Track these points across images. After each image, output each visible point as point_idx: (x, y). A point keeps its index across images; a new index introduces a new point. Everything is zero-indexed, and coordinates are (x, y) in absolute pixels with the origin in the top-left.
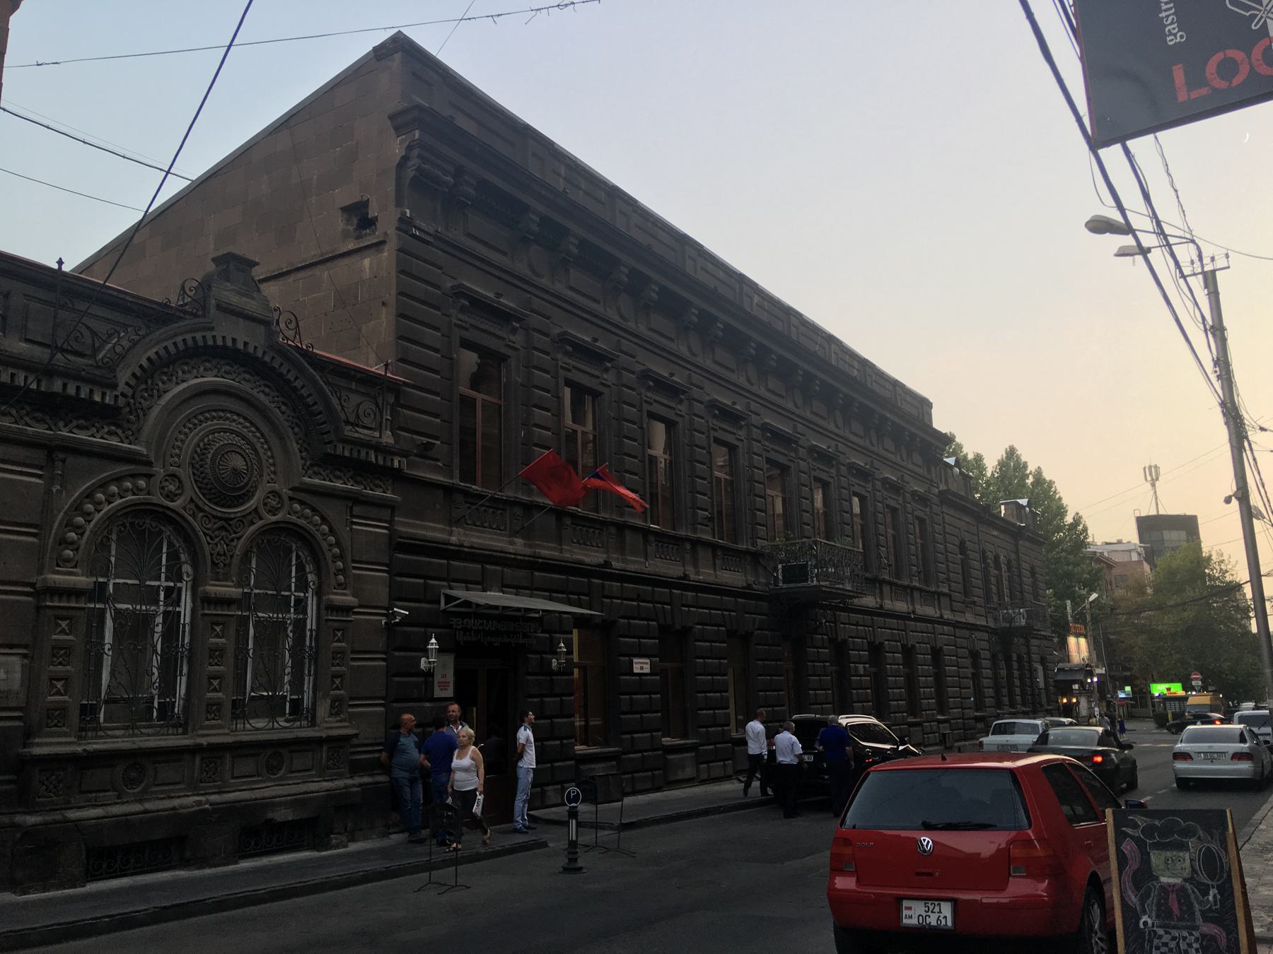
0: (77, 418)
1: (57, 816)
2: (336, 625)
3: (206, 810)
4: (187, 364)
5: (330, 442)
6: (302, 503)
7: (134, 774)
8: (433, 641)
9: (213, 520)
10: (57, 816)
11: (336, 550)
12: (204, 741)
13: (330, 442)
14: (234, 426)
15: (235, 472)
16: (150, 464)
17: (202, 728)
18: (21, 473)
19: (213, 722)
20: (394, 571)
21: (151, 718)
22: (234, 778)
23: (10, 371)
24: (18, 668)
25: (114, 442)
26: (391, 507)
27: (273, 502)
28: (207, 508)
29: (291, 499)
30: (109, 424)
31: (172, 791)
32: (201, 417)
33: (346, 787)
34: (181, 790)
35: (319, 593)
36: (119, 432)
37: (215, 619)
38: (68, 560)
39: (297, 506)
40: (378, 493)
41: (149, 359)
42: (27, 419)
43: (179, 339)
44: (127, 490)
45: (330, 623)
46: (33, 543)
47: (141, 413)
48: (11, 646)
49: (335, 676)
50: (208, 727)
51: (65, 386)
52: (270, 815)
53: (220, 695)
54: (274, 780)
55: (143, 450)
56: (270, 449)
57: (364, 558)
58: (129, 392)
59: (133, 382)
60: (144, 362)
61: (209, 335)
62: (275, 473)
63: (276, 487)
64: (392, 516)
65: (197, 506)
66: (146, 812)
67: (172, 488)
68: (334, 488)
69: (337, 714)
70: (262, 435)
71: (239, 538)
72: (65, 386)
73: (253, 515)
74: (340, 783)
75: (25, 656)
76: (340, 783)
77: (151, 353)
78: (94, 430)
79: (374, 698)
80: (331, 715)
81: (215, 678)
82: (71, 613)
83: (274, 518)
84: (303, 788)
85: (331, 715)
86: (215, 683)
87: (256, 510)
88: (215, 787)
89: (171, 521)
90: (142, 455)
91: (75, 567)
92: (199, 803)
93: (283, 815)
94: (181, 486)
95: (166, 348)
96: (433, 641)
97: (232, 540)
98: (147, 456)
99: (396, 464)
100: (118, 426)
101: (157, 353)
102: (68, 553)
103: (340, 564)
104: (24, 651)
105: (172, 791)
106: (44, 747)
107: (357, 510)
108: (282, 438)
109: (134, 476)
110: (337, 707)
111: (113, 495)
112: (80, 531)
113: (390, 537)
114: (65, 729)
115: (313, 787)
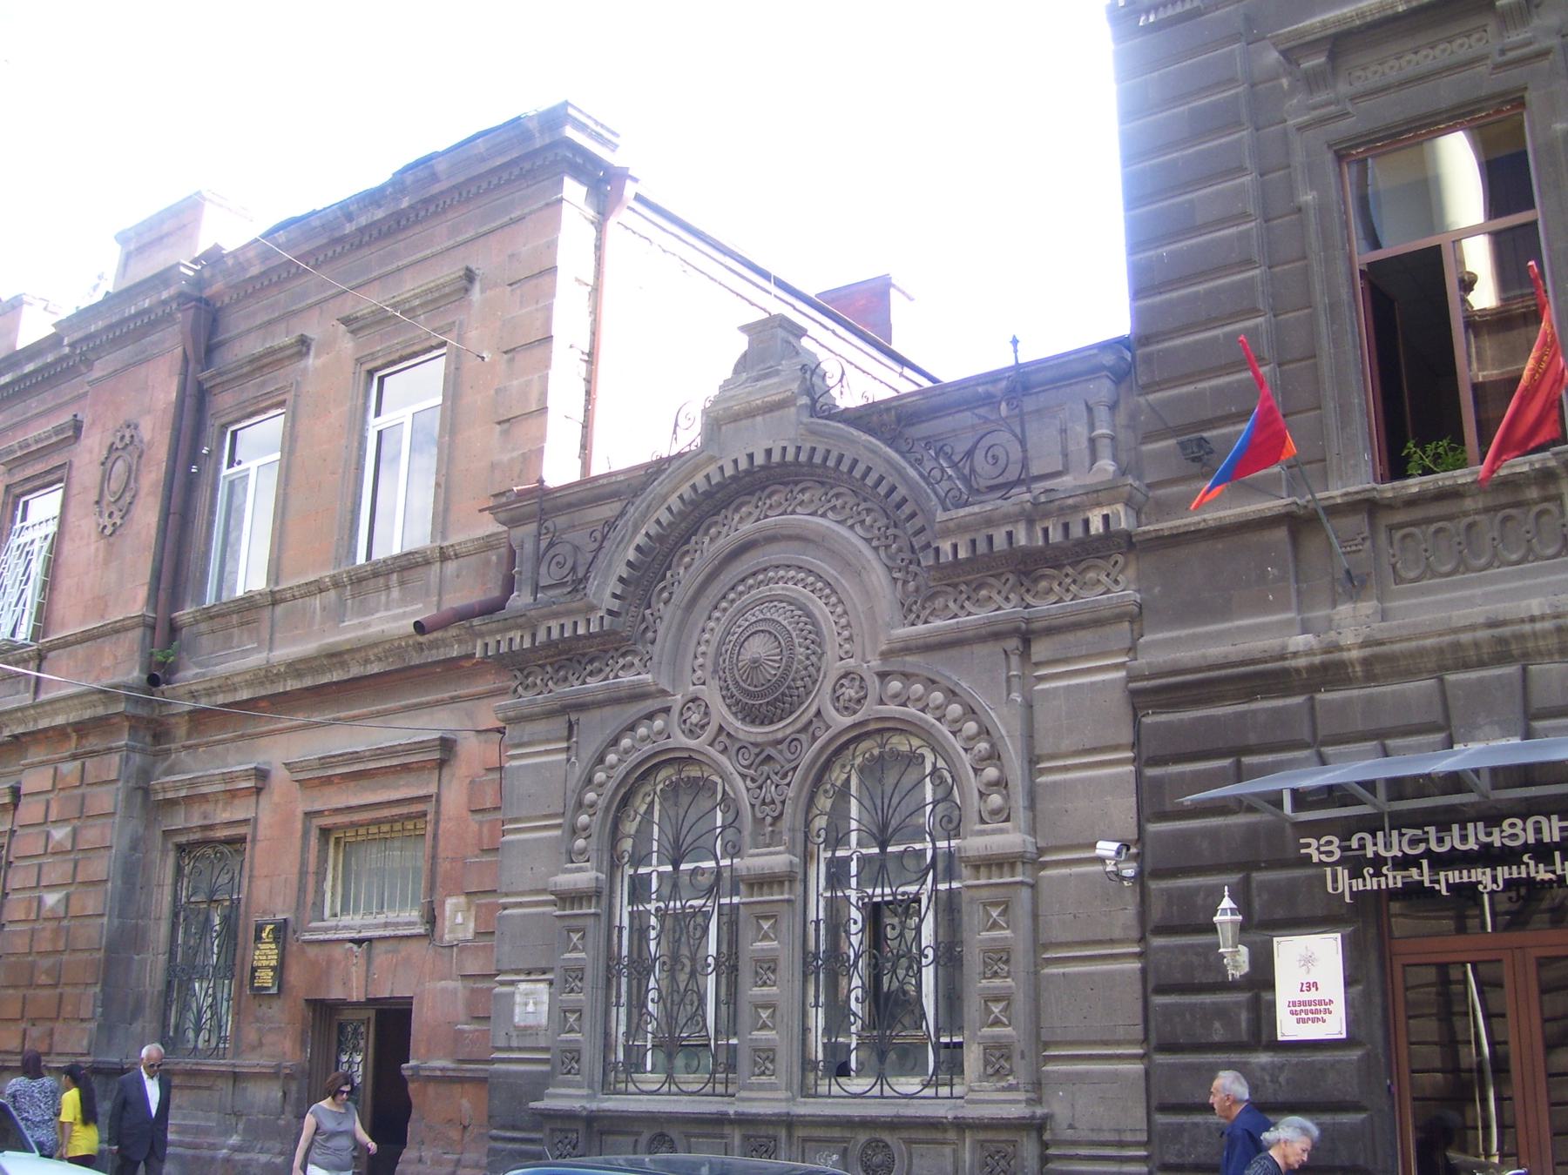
0: (591, 661)
5: (928, 545)
6: (906, 676)
8: (1227, 903)
14: (778, 589)
15: (756, 664)
16: (664, 693)
18: (547, 752)
24: (546, 998)
25: (627, 678)
27: (850, 693)
28: (741, 736)
29: (883, 676)
37: (759, 909)
39: (895, 685)
40: (1092, 597)
43: (673, 501)
50: (750, 1088)
55: (648, 677)
57: (1065, 745)
60: (631, 555)
62: (850, 639)
65: (729, 734)
67: (695, 718)
68: (959, 628)
71: (795, 769)
77: (640, 539)
79: (1118, 1043)
80: (986, 1077)
82: (579, 922)
83: (848, 720)
85: (986, 1077)
87: (818, 713)
96: (1227, 903)
97: (785, 776)
99: (1097, 526)
100: (634, 653)
101: (647, 534)
107: (1040, 650)
109: (650, 716)
110: (998, 1058)
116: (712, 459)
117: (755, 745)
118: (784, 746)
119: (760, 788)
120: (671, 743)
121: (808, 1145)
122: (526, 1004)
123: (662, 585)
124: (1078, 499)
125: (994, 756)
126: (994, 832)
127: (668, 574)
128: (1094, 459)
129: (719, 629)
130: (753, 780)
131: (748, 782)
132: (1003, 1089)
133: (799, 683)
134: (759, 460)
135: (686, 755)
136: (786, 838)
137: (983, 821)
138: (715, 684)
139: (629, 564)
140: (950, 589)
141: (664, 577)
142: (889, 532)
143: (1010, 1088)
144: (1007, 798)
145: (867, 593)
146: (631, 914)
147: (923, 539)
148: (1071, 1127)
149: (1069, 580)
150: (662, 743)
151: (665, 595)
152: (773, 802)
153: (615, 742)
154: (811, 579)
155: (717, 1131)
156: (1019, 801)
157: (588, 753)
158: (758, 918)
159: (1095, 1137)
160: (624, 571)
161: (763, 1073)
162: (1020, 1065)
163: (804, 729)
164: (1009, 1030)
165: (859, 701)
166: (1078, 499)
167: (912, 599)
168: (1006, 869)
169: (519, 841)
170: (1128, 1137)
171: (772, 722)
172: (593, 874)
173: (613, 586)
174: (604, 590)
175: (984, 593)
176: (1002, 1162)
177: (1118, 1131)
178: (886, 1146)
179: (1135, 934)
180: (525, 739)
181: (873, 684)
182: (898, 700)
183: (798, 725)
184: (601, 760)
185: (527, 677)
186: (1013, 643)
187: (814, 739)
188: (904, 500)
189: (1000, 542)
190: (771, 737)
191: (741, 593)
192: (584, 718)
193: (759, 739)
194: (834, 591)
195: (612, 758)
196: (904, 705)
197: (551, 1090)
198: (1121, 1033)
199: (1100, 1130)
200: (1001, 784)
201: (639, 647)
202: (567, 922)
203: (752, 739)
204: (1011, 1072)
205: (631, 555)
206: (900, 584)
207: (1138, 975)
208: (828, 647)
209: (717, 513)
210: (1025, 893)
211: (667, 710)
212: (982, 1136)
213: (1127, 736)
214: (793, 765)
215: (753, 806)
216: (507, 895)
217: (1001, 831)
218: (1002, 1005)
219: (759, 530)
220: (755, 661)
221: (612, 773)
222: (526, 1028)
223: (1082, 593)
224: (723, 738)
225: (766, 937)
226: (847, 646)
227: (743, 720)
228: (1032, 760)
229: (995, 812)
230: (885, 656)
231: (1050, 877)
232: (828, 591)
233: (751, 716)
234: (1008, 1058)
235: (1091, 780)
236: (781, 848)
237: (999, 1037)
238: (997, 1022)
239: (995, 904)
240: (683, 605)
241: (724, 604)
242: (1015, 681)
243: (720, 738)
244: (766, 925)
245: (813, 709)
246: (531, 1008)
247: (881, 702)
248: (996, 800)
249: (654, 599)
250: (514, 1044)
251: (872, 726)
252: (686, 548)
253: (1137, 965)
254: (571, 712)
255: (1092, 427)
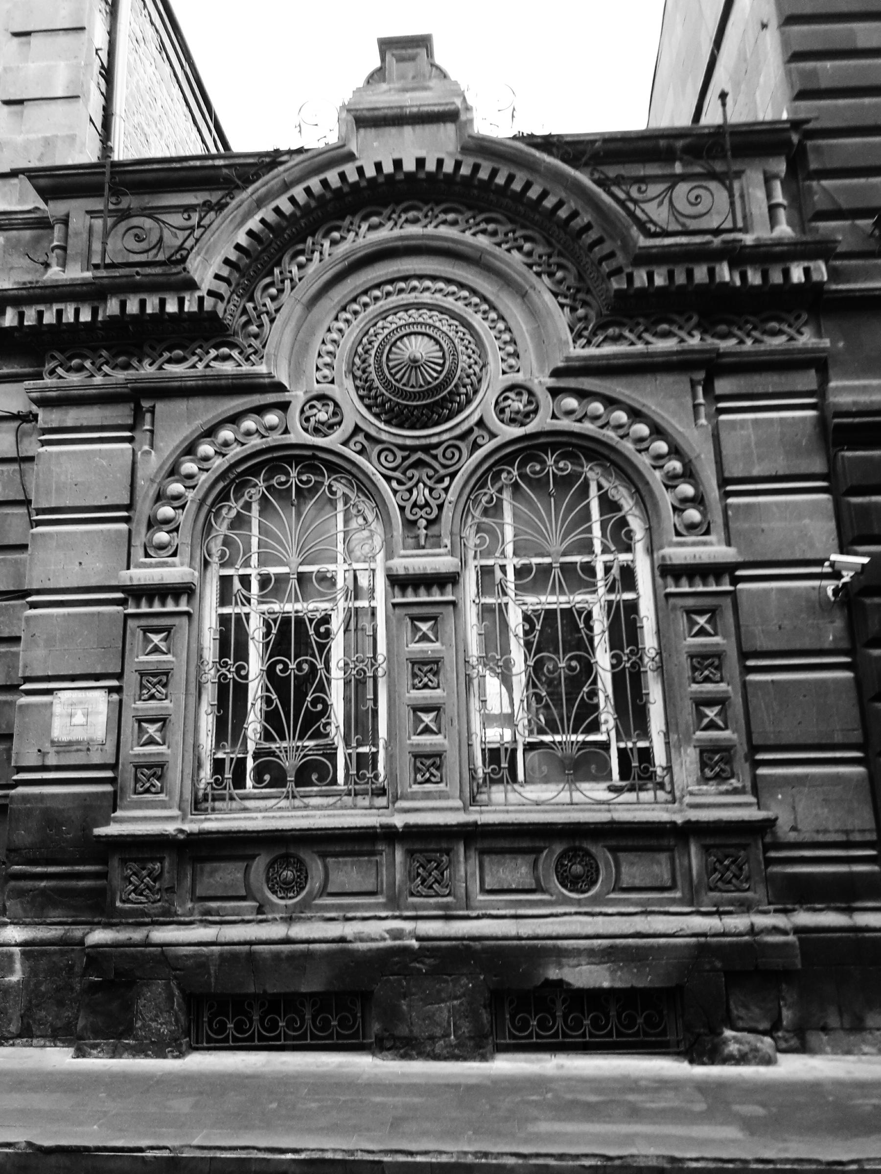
1: (137, 935)
2: (690, 602)
3: (406, 950)
4: (338, 229)
5: (617, 271)
6: (582, 395)
7: (288, 874)
9: (400, 454)
10: (137, 935)
11: (675, 465)
12: (399, 821)
13: (617, 271)
14: (426, 297)
15: (414, 364)
16: (280, 388)
17: (404, 797)
19: (429, 787)
20: (835, 483)
21: (334, 782)
22: (484, 891)
23: (55, 307)
25: (228, 367)
26: (819, 364)
27: (517, 404)
28: (384, 437)
29: (555, 392)
30: (217, 347)
31: (356, 907)
32: (365, 299)
33: (752, 930)
34: (377, 906)
35: (650, 551)
36: (235, 353)
37: (416, 611)
38: (161, 547)
39: (571, 403)
40: (778, 342)
41: (250, 233)
42: (105, 368)
43: (298, 192)
44: (248, 433)
45: (672, 601)
46: (118, 532)
47: (265, 318)
48: (97, 677)
49: (702, 702)
50: (413, 797)
51: (123, 305)
52: (553, 974)
53: (438, 739)
54: (579, 902)
55: (262, 369)
56: (502, 318)
57: (756, 472)
58: (223, 288)
59: (225, 272)
60: (242, 239)
61: (350, 169)
62: (516, 355)
63: (519, 378)
64: (824, 381)
65: (368, 436)
66: (287, 941)
67: (323, 416)
69: (720, 778)
70: (485, 299)
71: (453, 476)
72: (123, 305)
73: (477, 432)
74: (738, 922)
75: (111, 690)
76: (738, 922)
77: (254, 223)
78: (196, 358)
81: (427, 710)
84: (641, 924)
86: (427, 718)
87: (481, 423)
88: (438, 907)
89: (333, 469)
90: (261, 376)
91: (174, 555)
92: (397, 935)
93: (586, 976)
94: (337, 410)
95: (277, 210)
97: (441, 480)
98: (269, 375)
99: (797, 275)
100: (233, 346)
101: (263, 221)
102: (162, 536)
103: (687, 490)
104: (114, 683)
105: (356, 907)
106: (133, 822)
107: (722, 386)
108: (523, 295)
109: (260, 411)
110: (715, 762)
111: (226, 444)
112: (177, 504)
113: (822, 422)
114: (162, 797)
115: (659, 924)
116: (350, 157)
117: (402, 448)
118: (439, 452)
119: (410, 491)
120: (292, 438)
121: (487, 859)
122: (71, 716)
123: (268, 280)
124: (785, 248)
125: (689, 474)
126: (694, 544)
127: (277, 271)
128: (773, 222)
129: (352, 333)
130: (400, 482)
131: (394, 484)
132: (727, 793)
133: (463, 390)
134: (409, 166)
135: (308, 453)
136: (447, 541)
137: (678, 534)
138: (349, 383)
139: (238, 247)
140: (625, 320)
141: (271, 273)
142: (552, 260)
143: (735, 791)
144: (704, 514)
145: (533, 313)
146: (224, 620)
147: (613, 264)
148: (794, 829)
149: (750, 326)
150: (275, 438)
151: (273, 291)
152: (427, 504)
153: (210, 433)
154: (465, 293)
155: (366, 848)
156: (717, 518)
157: (170, 441)
158: (413, 619)
159: (821, 838)
160: (233, 256)
161: (428, 781)
162: (742, 767)
163: (463, 437)
164: (727, 734)
165: (527, 415)
166: (785, 248)
167: (580, 325)
168: (711, 580)
169: (58, 533)
170: (857, 837)
171: (424, 427)
172: (186, 569)
173: (216, 266)
174: (206, 270)
175: (665, 327)
176: (733, 867)
177: (847, 832)
178: (588, 854)
179: (844, 645)
180: (69, 423)
181: (546, 402)
182: (573, 417)
183: (458, 432)
184: (190, 450)
185: (70, 359)
186: (700, 376)
187: (476, 446)
188: (588, 227)
189: (701, 274)
190: (423, 442)
191: (376, 299)
192: (161, 407)
193: (408, 442)
194: (493, 308)
195: (206, 449)
196: (580, 421)
197: (119, 813)
198: (838, 738)
199: (826, 831)
200: (698, 501)
201: (240, 340)
202: (144, 622)
203: (400, 441)
204: (733, 776)
205: (242, 239)
206: (567, 310)
207: (853, 684)
208: (491, 358)
209: (343, 218)
210: (727, 602)
211: (284, 406)
212: (709, 841)
213: (818, 465)
214: (451, 470)
215: (402, 509)
216: (39, 592)
217: (705, 544)
218: (717, 709)
219: (401, 238)
220: (415, 361)
221: (206, 465)
222: (70, 743)
223: (766, 338)
224: (360, 438)
225: (425, 638)
226: (512, 361)
227: (387, 422)
228: (723, 481)
229: (692, 527)
230: (556, 373)
231: (748, 591)
232: (485, 307)
233: (399, 417)
234: (728, 761)
235: (787, 504)
236: (442, 550)
237: (717, 740)
238: (712, 726)
239: (701, 612)
240: (305, 299)
241: (356, 307)
242: (702, 410)
243: (356, 439)
244: (424, 627)
245: (475, 418)
246: (79, 719)
247: (554, 417)
248: (693, 515)
249: (258, 294)
250: (52, 761)
251: (542, 440)
252: (300, 247)
253: (849, 674)
254: (139, 400)
255: (769, 195)
